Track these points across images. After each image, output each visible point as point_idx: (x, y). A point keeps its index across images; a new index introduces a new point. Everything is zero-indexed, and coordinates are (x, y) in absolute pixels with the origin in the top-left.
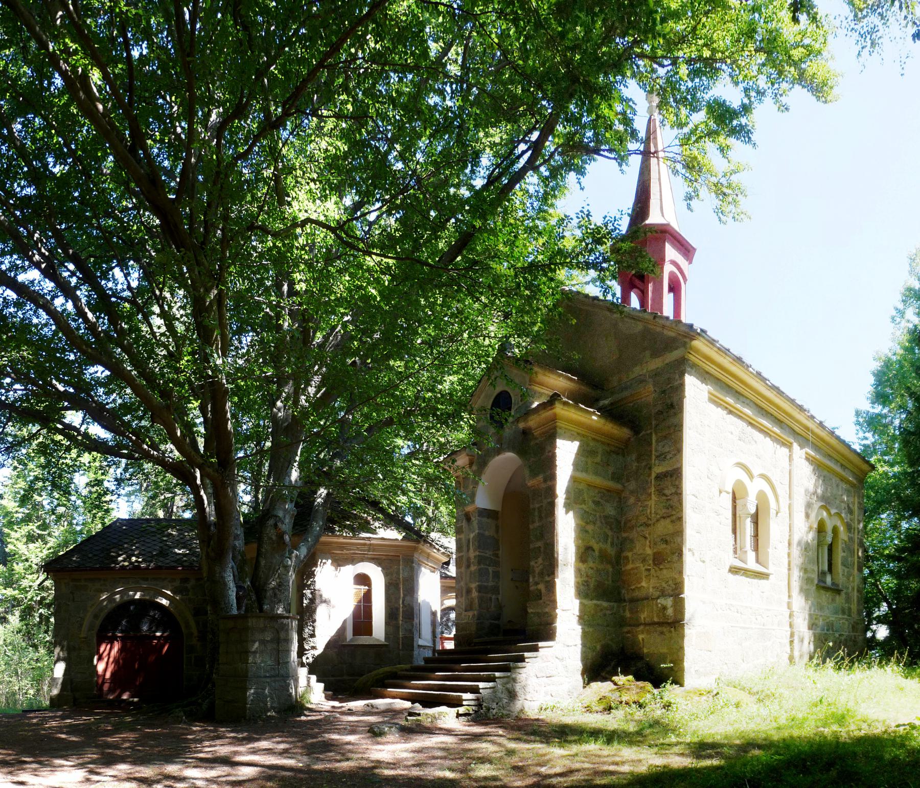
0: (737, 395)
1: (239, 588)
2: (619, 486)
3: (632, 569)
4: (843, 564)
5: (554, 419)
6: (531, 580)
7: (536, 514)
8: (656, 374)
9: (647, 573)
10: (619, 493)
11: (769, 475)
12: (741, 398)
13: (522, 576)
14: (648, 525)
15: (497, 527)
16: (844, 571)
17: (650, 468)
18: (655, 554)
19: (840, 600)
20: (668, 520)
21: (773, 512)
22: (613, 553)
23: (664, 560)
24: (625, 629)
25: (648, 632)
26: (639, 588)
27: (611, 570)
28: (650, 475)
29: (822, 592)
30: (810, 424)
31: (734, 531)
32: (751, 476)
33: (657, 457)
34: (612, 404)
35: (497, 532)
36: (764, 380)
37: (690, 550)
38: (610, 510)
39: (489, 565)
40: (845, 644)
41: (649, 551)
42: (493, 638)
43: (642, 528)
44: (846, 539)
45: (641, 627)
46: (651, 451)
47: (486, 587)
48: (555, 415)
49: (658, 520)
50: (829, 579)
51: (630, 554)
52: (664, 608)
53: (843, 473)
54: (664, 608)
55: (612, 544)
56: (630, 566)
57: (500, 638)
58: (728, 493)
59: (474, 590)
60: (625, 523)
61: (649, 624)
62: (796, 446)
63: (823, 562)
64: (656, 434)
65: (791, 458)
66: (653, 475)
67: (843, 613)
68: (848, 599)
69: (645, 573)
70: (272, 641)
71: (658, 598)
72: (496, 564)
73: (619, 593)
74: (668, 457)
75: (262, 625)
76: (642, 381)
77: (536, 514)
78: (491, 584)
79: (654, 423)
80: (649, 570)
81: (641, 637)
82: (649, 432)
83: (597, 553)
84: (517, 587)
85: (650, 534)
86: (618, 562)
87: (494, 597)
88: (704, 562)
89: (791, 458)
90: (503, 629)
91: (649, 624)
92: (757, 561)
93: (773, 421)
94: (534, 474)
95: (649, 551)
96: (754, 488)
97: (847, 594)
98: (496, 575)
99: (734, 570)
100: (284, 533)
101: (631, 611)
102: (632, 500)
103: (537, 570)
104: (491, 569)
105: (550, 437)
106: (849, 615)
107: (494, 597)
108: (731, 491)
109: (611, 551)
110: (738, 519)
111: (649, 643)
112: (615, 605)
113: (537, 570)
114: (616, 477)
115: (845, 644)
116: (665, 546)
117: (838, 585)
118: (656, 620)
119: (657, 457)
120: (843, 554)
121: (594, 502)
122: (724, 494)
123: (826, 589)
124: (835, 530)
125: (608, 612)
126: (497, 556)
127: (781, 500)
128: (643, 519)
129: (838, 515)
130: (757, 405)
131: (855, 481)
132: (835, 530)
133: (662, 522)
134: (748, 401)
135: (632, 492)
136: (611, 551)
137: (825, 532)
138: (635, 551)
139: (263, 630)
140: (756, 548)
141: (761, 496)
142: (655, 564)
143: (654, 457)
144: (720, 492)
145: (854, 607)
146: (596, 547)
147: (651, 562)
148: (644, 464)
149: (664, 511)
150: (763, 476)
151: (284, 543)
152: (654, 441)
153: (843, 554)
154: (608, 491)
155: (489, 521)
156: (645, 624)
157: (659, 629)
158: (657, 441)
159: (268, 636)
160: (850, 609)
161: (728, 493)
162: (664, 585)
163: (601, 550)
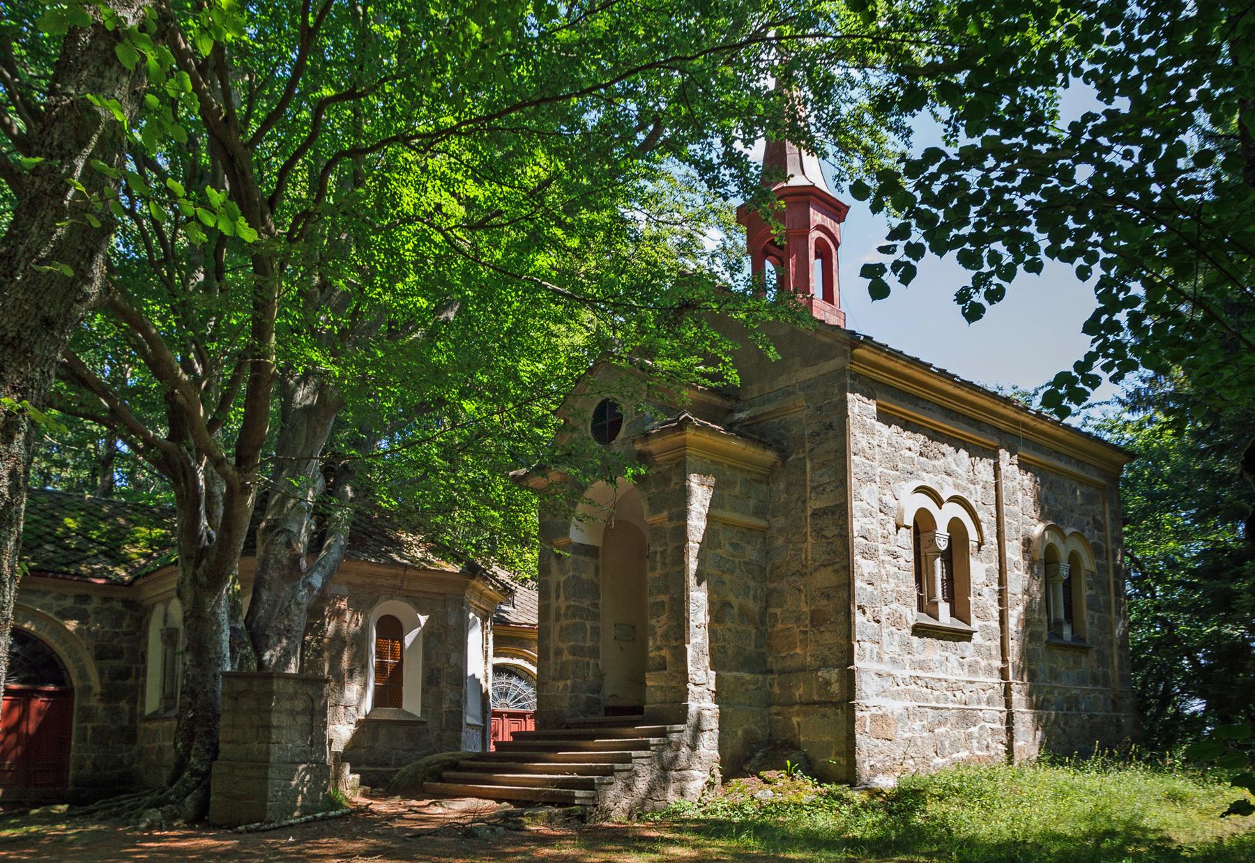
0: (914, 400)
1: (233, 629)
2: (763, 523)
3: (782, 630)
4: (1090, 607)
5: (683, 445)
6: (651, 643)
7: (658, 558)
8: (808, 386)
9: (802, 636)
10: (763, 531)
11: (964, 495)
12: (920, 403)
13: (634, 635)
14: (803, 575)
15: (597, 569)
16: (1093, 617)
17: (804, 502)
18: (813, 612)
19: (1088, 663)
20: (830, 569)
21: (973, 544)
22: (757, 609)
23: (825, 620)
24: (774, 709)
25: (806, 714)
26: (792, 656)
27: (754, 631)
28: (804, 511)
29: (1058, 652)
30: (1022, 418)
31: (918, 579)
32: (939, 502)
33: (813, 489)
34: (750, 418)
35: (597, 575)
36: (951, 377)
37: (860, 607)
38: (752, 553)
39: (587, 619)
40: (1064, 746)
41: (805, 608)
42: (591, 718)
43: (794, 577)
44: (1093, 569)
45: (796, 708)
46: (805, 480)
47: (582, 648)
48: (685, 440)
49: (816, 570)
50: (1067, 632)
51: (778, 611)
52: (828, 683)
53: (1083, 474)
54: (828, 683)
55: (755, 598)
56: (780, 626)
57: (601, 717)
58: (908, 527)
59: (566, 652)
60: (771, 572)
61: (808, 704)
62: (1004, 455)
63: (1056, 607)
64: (811, 460)
65: (996, 468)
66: (809, 512)
67: (1095, 680)
68: (1103, 660)
69: (800, 637)
70: (303, 712)
71: (818, 670)
72: (596, 616)
73: (765, 662)
74: (828, 490)
75: (291, 690)
76: (790, 394)
77: (658, 558)
78: (588, 644)
79: (808, 446)
80: (806, 633)
81: (795, 720)
82: (801, 456)
83: (736, 609)
84: (621, 649)
85: (805, 586)
86: (762, 622)
87: (592, 661)
88: (878, 622)
89: (996, 468)
90: (612, 704)
91: (808, 704)
92: (953, 614)
93: (969, 424)
94: (655, 507)
95: (805, 608)
96: (943, 517)
97: (1100, 653)
98: (596, 632)
99: (919, 630)
100: (300, 556)
101: (781, 685)
102: (780, 541)
103: (660, 632)
104: (588, 625)
105: (680, 469)
106: (1106, 684)
107: (592, 661)
108: (911, 524)
109: (754, 606)
110: (923, 559)
111: (809, 730)
112: (760, 677)
113: (660, 632)
114: (759, 512)
115: (1064, 746)
116: (826, 602)
117: (1083, 640)
118: (816, 698)
119: (813, 489)
120: (1089, 592)
121: (732, 544)
122: (902, 530)
123: (1064, 647)
124: (1074, 558)
125: (752, 687)
126: (596, 606)
127: (984, 526)
128: (794, 566)
129: (1079, 535)
130: (943, 408)
131: (1103, 481)
132: (1074, 558)
133: (823, 571)
134: (930, 406)
135: (780, 531)
136: (754, 606)
137: (1057, 562)
138: (786, 607)
139: (292, 698)
140: (950, 597)
141: (956, 526)
142: (813, 626)
143: (809, 490)
144: (898, 528)
145: (1114, 671)
146: (735, 602)
147: (808, 622)
148: (796, 496)
149: (824, 557)
150: (955, 499)
151: (300, 570)
152: (808, 469)
153: (1089, 592)
154: (750, 529)
155: (586, 559)
156: (801, 704)
157: (823, 710)
158: (813, 469)
159: (299, 705)
160: (1105, 674)
161: (908, 527)
162: (826, 653)
163: (741, 607)
